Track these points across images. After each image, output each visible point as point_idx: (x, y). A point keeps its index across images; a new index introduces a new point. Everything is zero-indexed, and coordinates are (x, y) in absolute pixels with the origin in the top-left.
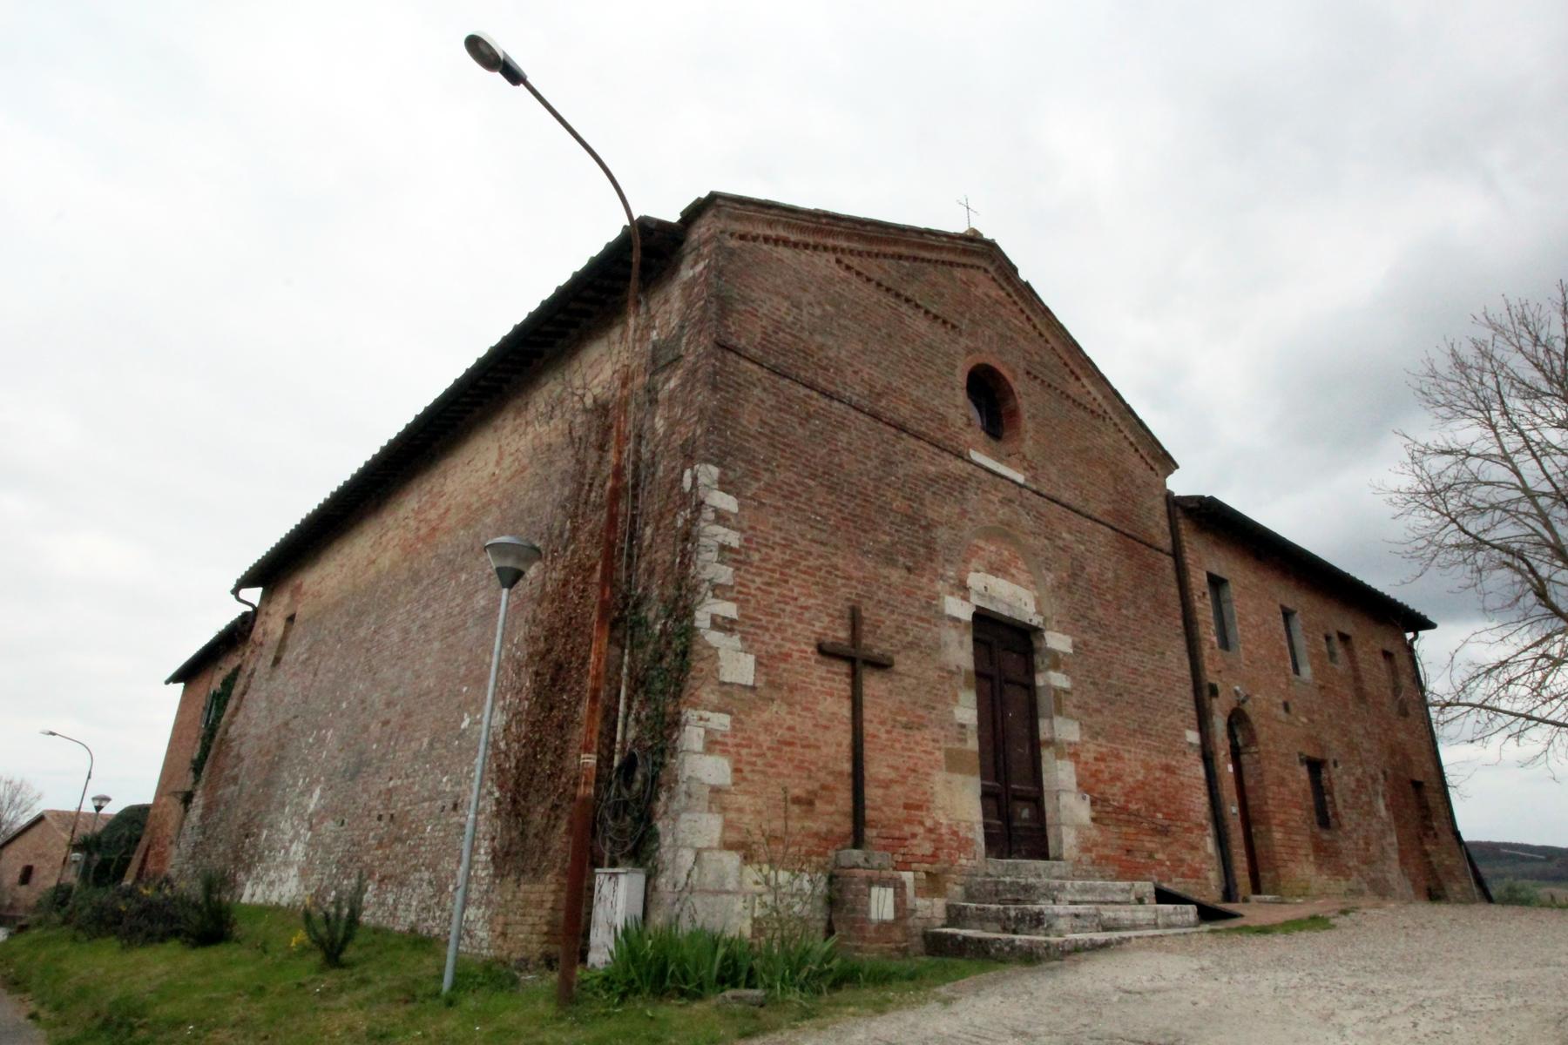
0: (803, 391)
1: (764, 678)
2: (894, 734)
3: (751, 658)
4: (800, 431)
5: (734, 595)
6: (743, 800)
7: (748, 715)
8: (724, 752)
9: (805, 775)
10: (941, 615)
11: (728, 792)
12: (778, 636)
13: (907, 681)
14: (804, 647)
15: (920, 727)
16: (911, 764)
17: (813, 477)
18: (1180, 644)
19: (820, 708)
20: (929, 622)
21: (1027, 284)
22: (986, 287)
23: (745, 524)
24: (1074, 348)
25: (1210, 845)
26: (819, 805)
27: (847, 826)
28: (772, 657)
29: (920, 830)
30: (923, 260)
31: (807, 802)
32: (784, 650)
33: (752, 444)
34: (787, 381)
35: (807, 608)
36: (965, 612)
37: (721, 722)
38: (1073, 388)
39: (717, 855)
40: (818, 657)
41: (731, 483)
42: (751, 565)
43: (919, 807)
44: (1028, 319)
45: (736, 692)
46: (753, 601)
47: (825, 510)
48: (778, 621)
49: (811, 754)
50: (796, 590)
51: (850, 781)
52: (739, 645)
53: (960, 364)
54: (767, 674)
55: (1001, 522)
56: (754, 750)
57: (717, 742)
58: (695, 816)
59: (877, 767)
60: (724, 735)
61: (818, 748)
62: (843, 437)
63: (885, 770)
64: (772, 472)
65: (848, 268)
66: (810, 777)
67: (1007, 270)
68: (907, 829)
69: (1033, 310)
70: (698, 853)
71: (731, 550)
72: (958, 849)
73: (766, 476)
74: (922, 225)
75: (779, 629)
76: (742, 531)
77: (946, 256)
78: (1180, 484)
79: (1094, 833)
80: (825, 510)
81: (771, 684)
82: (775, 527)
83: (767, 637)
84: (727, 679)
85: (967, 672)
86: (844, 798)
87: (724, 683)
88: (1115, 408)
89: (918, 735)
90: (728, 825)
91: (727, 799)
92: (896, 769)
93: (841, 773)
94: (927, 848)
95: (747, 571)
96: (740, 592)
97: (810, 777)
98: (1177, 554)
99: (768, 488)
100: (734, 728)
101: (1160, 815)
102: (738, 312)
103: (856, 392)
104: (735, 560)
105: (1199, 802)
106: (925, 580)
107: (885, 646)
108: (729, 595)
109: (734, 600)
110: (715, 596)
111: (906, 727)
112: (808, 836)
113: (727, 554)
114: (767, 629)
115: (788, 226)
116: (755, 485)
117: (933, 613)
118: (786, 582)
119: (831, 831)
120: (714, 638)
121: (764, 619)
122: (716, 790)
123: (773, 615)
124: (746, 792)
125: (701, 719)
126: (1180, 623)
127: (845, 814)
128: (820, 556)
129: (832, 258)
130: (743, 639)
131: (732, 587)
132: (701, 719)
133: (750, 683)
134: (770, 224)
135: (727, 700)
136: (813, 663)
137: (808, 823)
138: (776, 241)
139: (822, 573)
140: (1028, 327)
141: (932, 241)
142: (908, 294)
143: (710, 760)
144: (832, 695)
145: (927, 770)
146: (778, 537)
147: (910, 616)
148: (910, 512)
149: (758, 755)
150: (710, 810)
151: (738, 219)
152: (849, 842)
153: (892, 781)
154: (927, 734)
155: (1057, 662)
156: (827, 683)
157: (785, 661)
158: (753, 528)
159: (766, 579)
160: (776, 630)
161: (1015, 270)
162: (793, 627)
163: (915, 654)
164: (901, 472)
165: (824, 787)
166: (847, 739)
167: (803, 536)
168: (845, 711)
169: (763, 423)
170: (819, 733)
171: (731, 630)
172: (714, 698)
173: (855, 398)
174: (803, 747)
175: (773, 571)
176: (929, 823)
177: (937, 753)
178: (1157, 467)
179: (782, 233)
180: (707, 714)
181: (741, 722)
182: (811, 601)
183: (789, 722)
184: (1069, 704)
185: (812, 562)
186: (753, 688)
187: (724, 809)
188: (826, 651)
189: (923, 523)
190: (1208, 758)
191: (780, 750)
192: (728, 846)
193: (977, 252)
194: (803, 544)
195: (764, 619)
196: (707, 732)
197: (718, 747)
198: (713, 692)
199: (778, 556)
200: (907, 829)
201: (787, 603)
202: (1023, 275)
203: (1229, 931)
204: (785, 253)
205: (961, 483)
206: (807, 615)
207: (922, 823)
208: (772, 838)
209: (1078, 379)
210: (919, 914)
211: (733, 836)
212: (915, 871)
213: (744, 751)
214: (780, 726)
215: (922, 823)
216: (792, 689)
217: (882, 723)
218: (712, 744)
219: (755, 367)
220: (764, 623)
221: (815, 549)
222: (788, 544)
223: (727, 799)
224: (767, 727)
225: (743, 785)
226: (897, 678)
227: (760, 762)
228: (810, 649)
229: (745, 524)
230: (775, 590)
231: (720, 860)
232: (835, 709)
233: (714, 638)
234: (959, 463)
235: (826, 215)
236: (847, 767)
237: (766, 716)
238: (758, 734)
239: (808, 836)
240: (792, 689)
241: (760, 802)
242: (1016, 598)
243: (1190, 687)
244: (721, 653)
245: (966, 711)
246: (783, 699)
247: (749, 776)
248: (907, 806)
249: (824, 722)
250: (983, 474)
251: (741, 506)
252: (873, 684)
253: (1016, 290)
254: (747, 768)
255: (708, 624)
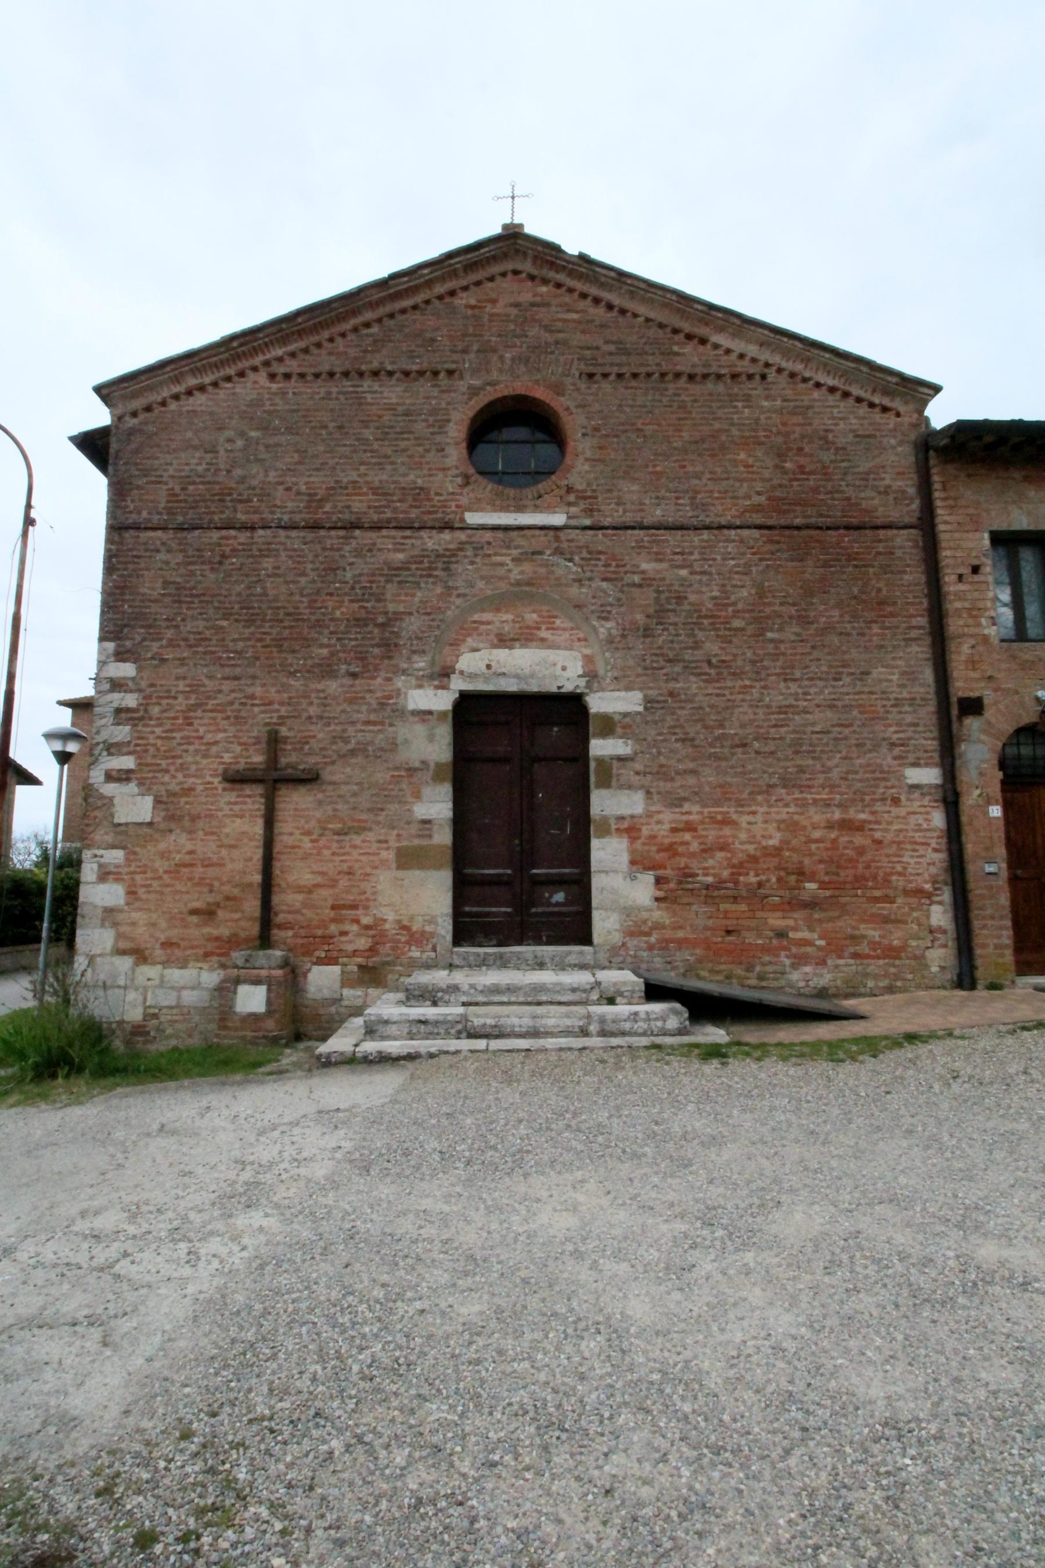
0: (215, 535)
1: (163, 814)
2: (321, 843)
3: (149, 800)
4: (212, 576)
5: (131, 748)
6: (135, 915)
7: (145, 847)
8: (117, 880)
9: (206, 889)
10: (401, 713)
11: (121, 911)
12: (180, 775)
13: (344, 789)
14: (209, 779)
15: (360, 829)
16: (345, 867)
17: (226, 617)
18: (921, 651)
19: (226, 830)
20: (382, 723)
21: (583, 258)
22: (509, 294)
23: (143, 684)
24: (683, 302)
25: (940, 915)
26: (221, 914)
27: (255, 930)
28: (171, 794)
29: (355, 928)
30: (403, 311)
31: (208, 914)
32: (186, 786)
33: (154, 608)
34: (197, 533)
35: (216, 743)
36: (443, 701)
37: (115, 856)
38: (690, 357)
39: (108, 959)
40: (227, 785)
41: (127, 652)
42: (151, 719)
43: (354, 907)
44: (597, 301)
45: (131, 830)
46: (152, 750)
47: (241, 645)
48: (180, 761)
49: (211, 872)
50: (202, 730)
51: (259, 891)
52: (136, 790)
53: (456, 416)
54: (167, 810)
55: (518, 583)
56: (149, 875)
57: (109, 873)
58: (89, 932)
59: (296, 873)
60: (117, 866)
61: (224, 865)
62: (268, 563)
63: (309, 876)
64: (177, 627)
65: (287, 376)
66: (211, 891)
67: (548, 253)
68: (333, 928)
69: (602, 285)
70: (91, 960)
71: (128, 710)
72: (408, 943)
73: (169, 634)
74: (383, 273)
75: (182, 768)
76: (140, 691)
77: (440, 289)
78: (940, 414)
79: (660, 915)
80: (241, 645)
81: (171, 818)
82: (177, 678)
83: (167, 778)
84: (123, 821)
85: (438, 765)
86: (252, 905)
87: (120, 825)
88: (786, 354)
89: (357, 840)
90: (119, 936)
91: (120, 917)
92: (323, 874)
93: (250, 885)
94: (363, 943)
95: (147, 725)
96: (137, 745)
97: (211, 891)
98: (927, 524)
99: (172, 644)
100: (127, 859)
101: (811, 886)
102: (138, 487)
103: (290, 507)
104: (132, 719)
105: (928, 862)
106: (379, 680)
107: (312, 760)
108: (125, 750)
109: (129, 753)
110: (110, 754)
111: (338, 833)
112: (208, 940)
113: (123, 715)
114: (167, 771)
115: (193, 372)
116: (155, 645)
117: (391, 710)
118: (191, 724)
119: (235, 935)
120: (109, 789)
121: (164, 763)
122: (109, 911)
123: (173, 757)
124: (140, 909)
125: (96, 856)
126: (923, 621)
127: (251, 919)
128: (233, 691)
129: (262, 378)
130: (140, 784)
131: (129, 742)
132: (96, 856)
133: (148, 820)
134: (177, 380)
135: (120, 838)
136: (220, 791)
137: (206, 930)
138: (189, 393)
139: (236, 706)
140: (600, 311)
141: (404, 283)
142: (375, 365)
143: (102, 888)
144: (242, 817)
145: (368, 870)
146: (182, 685)
147: (353, 723)
148: (363, 614)
149: (153, 879)
150: (102, 926)
151: (134, 395)
152: (257, 943)
153: (317, 886)
154: (370, 836)
155: (609, 726)
156: (236, 808)
157: (187, 795)
158: (152, 685)
159: (168, 727)
160: (177, 770)
161: (555, 249)
162: (197, 763)
163: (360, 759)
164: (349, 575)
165: (228, 898)
166: (259, 853)
167: (210, 677)
168: (258, 828)
169: (166, 584)
170: (224, 852)
171: (128, 780)
172: (109, 838)
173: (286, 517)
174: (204, 866)
175: (175, 718)
176: (366, 920)
177: (384, 854)
178: (897, 404)
179: (192, 381)
180: (96, 852)
181: (135, 853)
182: (221, 735)
183: (189, 846)
184: (627, 773)
185: (221, 699)
186: (150, 824)
187: (115, 924)
188: (236, 779)
189: (381, 619)
190: (951, 799)
191: (178, 872)
192: (123, 952)
193: (513, 251)
194: (210, 685)
195: (164, 763)
196: (100, 866)
197: (111, 877)
198: (106, 833)
199: (181, 703)
200: (333, 928)
201: (189, 744)
202: (571, 248)
203: (813, 1051)
204: (200, 400)
205: (448, 558)
206: (214, 749)
207: (357, 921)
208: (167, 944)
209: (703, 341)
210: (345, 1003)
211: (123, 945)
212: (344, 965)
213: (138, 878)
214: (179, 852)
215: (357, 921)
216: (194, 818)
217: (308, 833)
218: (105, 875)
219: (159, 533)
220: (164, 766)
221: (227, 686)
222: (195, 688)
223: (120, 917)
224: (164, 855)
225: (138, 904)
226: (330, 788)
227: (155, 884)
228: (216, 780)
229: (143, 684)
230: (178, 735)
231: (112, 963)
232: (246, 828)
233: (109, 789)
234: (447, 536)
235: (233, 338)
236: (258, 878)
237: (162, 846)
238: (153, 861)
239: (208, 940)
240: (194, 818)
241: (154, 916)
242: (546, 666)
243: (932, 707)
244: (116, 801)
245: (437, 806)
246: (183, 829)
247: (144, 896)
248: (333, 907)
249: (232, 842)
250: (488, 536)
251: (139, 669)
252: (295, 802)
253: (571, 273)
254: (141, 891)
255: (102, 778)
